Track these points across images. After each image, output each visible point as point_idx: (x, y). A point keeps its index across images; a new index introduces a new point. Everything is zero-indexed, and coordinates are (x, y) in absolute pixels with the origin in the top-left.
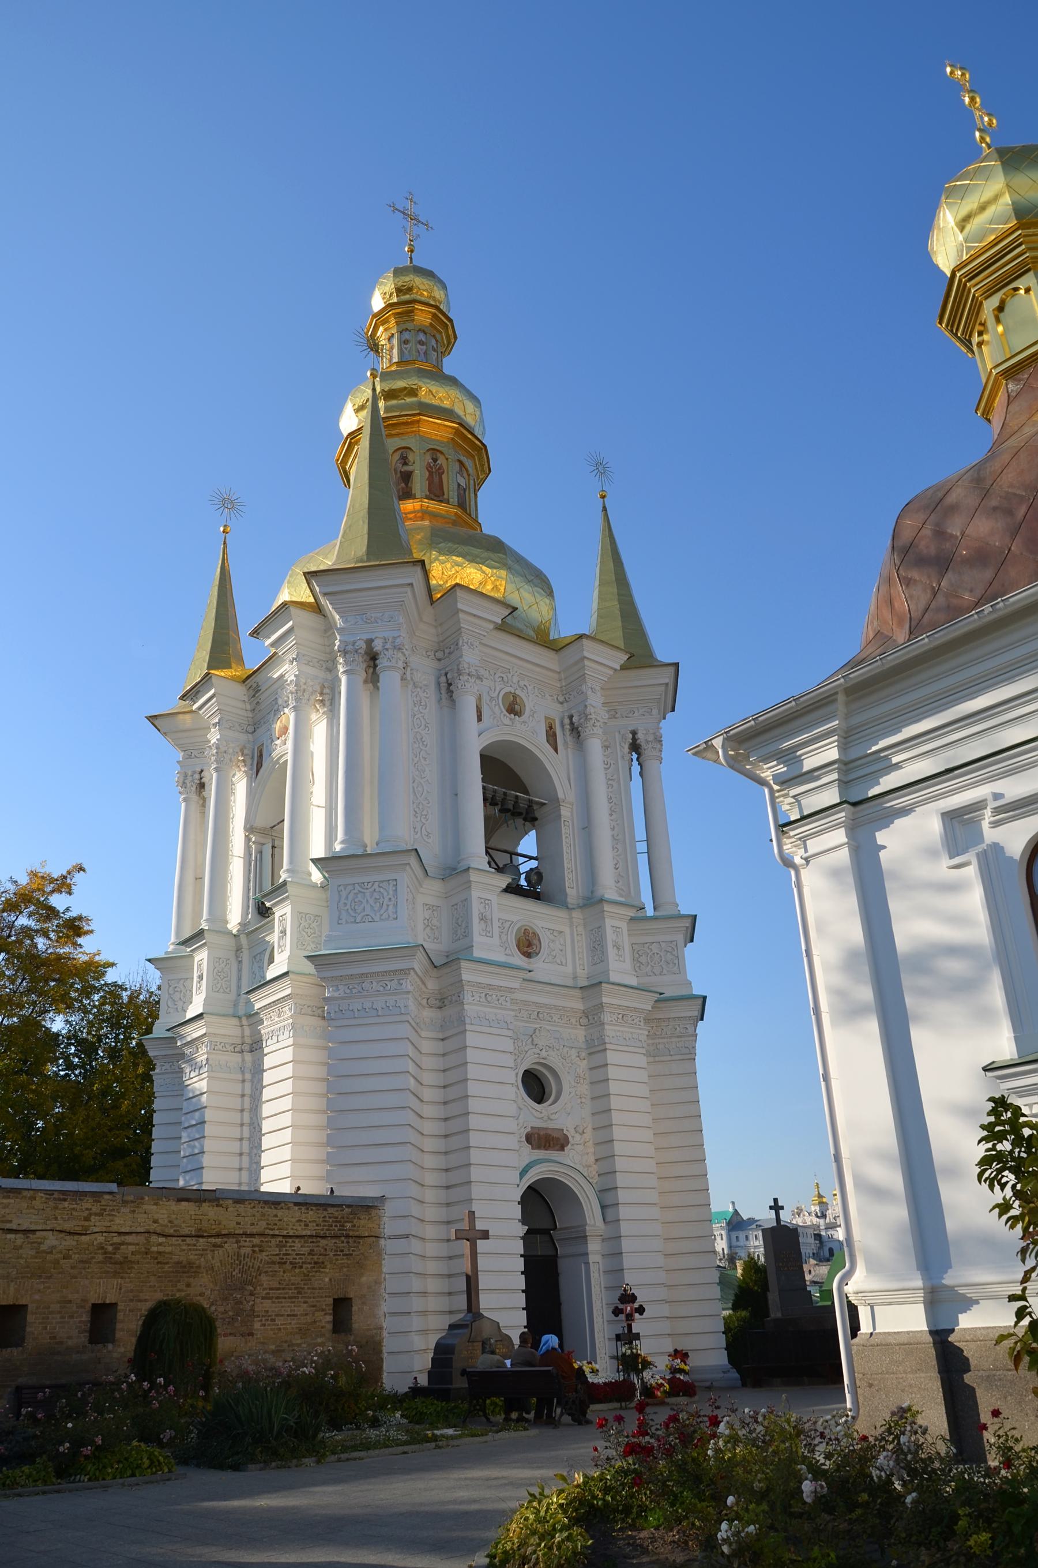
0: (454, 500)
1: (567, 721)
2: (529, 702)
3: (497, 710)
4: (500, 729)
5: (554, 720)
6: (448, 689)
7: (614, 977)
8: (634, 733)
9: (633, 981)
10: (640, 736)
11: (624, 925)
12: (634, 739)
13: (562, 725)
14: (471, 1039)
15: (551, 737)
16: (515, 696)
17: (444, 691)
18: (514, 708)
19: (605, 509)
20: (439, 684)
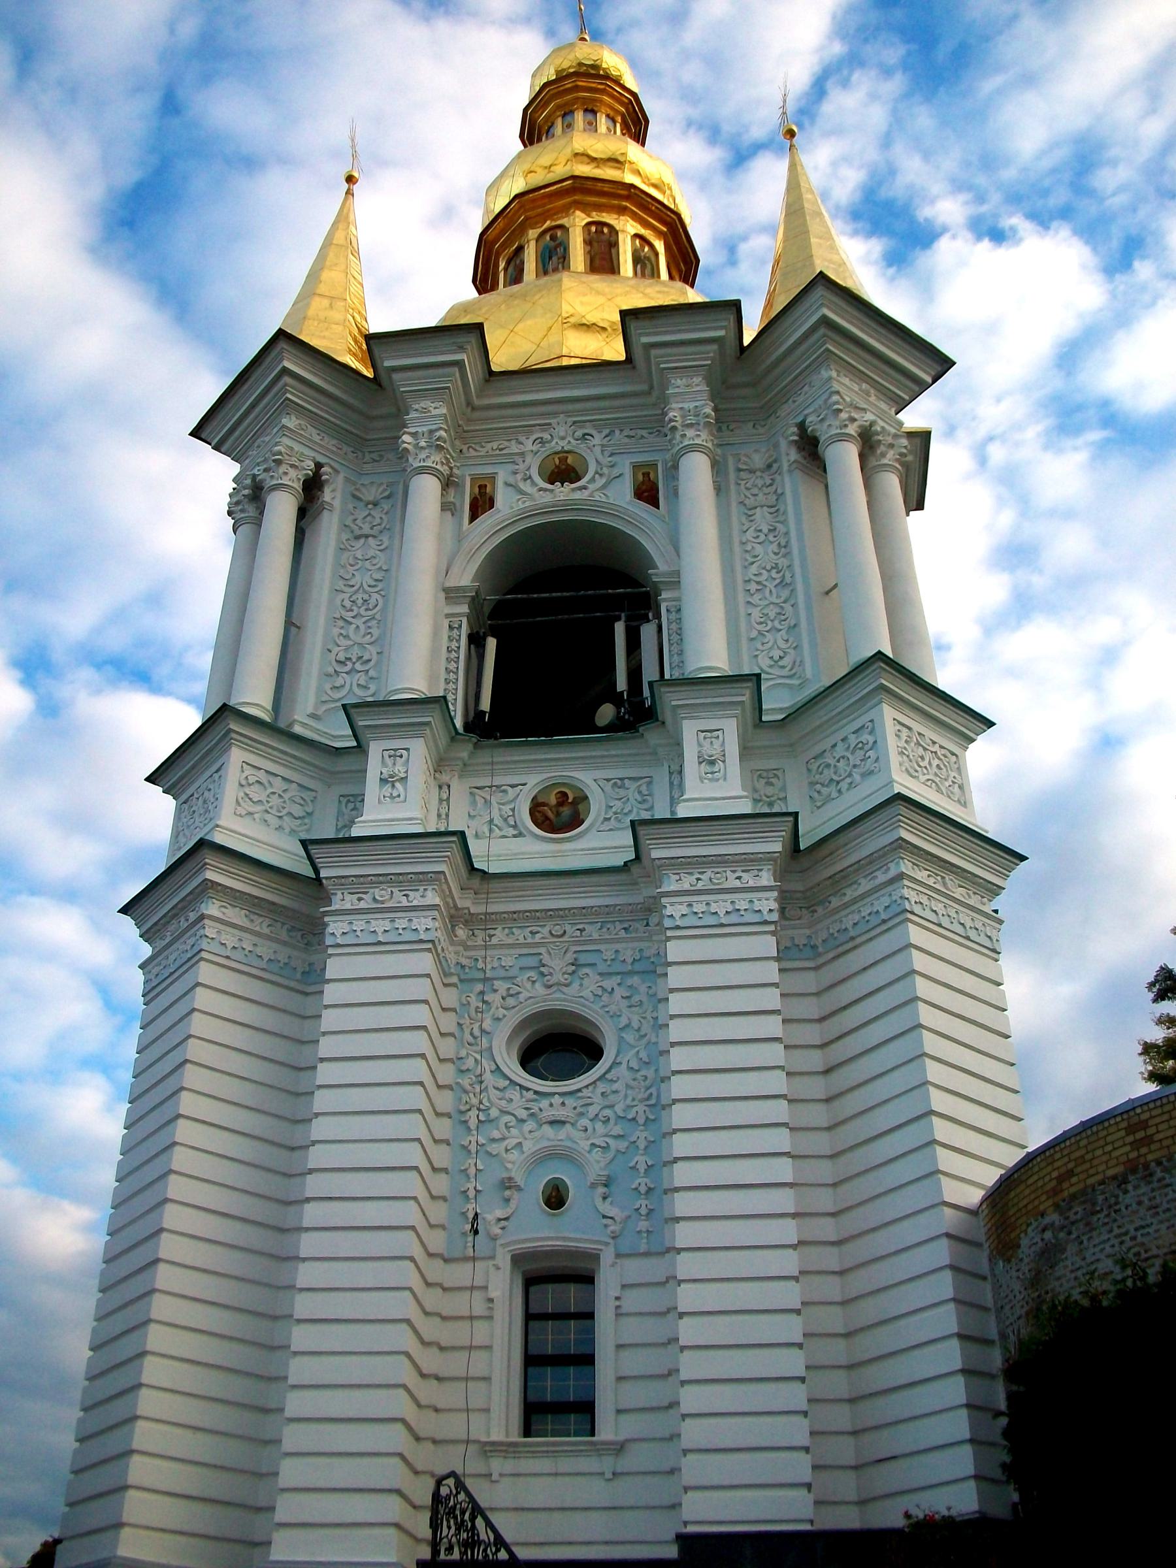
2: (593, 454)
3: (526, 487)
15: (647, 493)
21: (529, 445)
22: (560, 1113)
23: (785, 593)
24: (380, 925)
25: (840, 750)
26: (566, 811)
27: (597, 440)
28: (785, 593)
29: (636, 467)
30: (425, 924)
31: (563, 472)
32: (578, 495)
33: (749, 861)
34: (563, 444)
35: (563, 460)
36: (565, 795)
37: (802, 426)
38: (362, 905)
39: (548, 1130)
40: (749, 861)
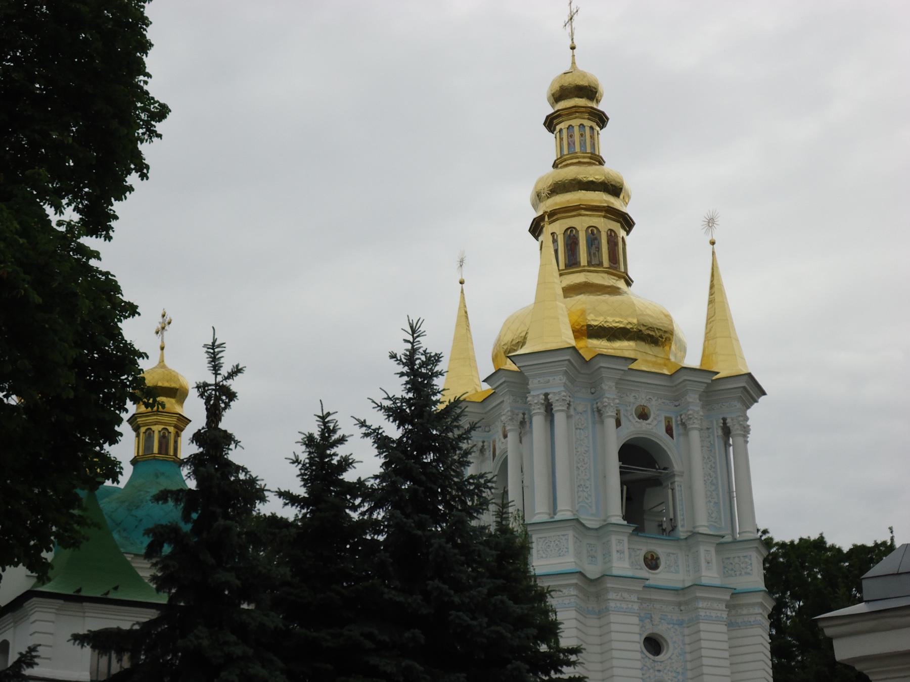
0: (606, 263)
1: (679, 418)
3: (631, 418)
4: (633, 428)
5: (671, 418)
6: (599, 413)
7: (704, 581)
8: (724, 420)
9: (717, 582)
10: (729, 422)
11: (712, 550)
12: (725, 423)
13: (676, 421)
14: (613, 618)
15: (669, 431)
16: (644, 407)
17: (596, 414)
18: (643, 415)
19: (713, 253)
20: (593, 411)
21: (632, 400)
22: (660, 668)
23: (713, 487)
24: (624, 606)
25: (737, 560)
26: (654, 562)
27: (654, 402)
28: (713, 487)
29: (666, 418)
30: (636, 607)
31: (643, 415)
32: (650, 427)
33: (720, 600)
34: (643, 403)
35: (644, 410)
36: (652, 556)
37: (724, 420)
38: (618, 597)
39: (657, 673)
40: (720, 600)
